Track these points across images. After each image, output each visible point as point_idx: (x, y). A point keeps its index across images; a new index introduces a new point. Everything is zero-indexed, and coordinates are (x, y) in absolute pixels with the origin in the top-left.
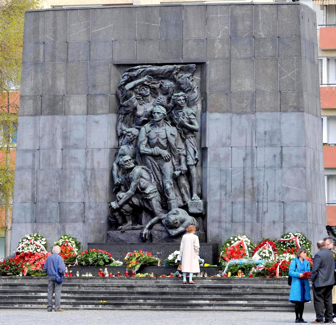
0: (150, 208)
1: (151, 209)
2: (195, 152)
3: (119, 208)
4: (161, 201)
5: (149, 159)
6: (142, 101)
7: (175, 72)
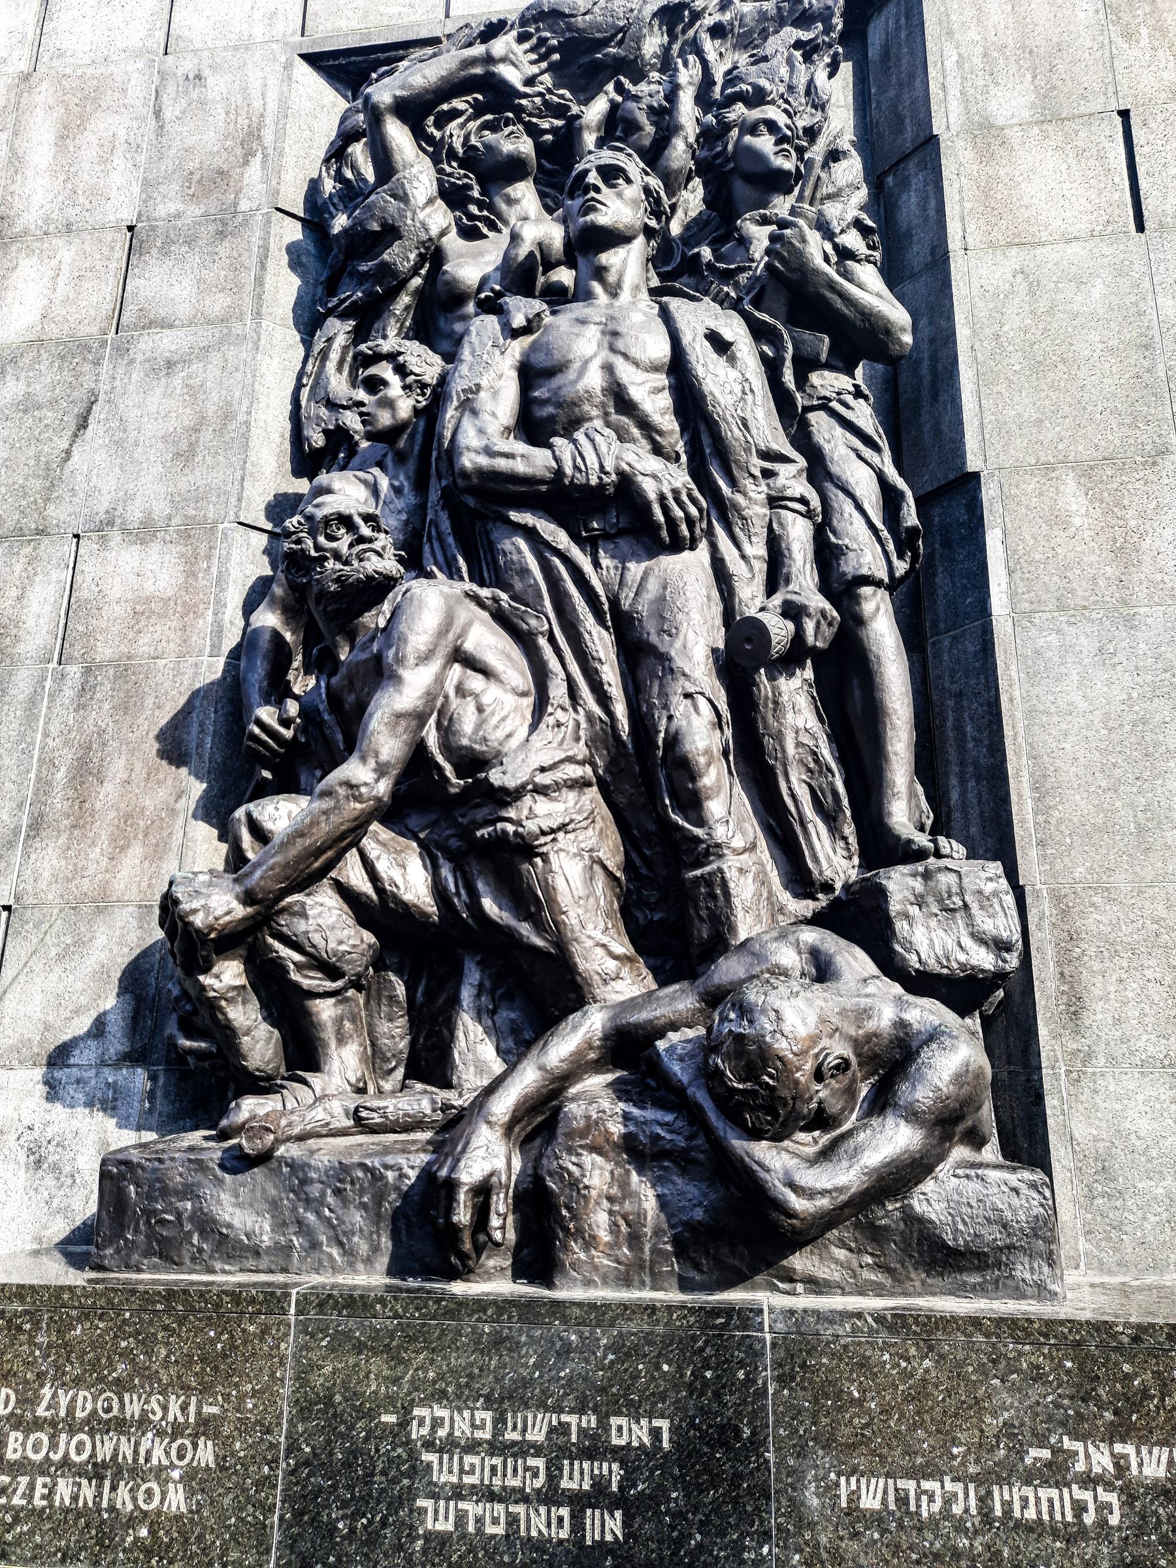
0: (525, 929)
1: (540, 926)
2: (890, 497)
3: (244, 919)
4: (628, 866)
5: (531, 534)
6: (481, 205)
7: (708, 21)
